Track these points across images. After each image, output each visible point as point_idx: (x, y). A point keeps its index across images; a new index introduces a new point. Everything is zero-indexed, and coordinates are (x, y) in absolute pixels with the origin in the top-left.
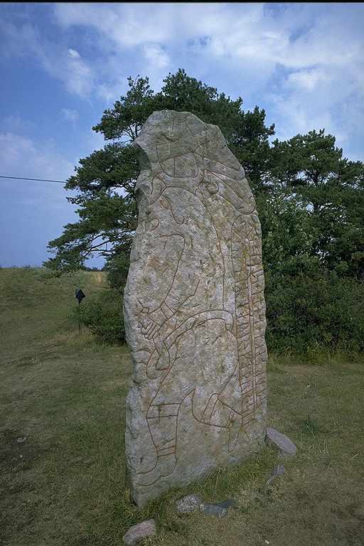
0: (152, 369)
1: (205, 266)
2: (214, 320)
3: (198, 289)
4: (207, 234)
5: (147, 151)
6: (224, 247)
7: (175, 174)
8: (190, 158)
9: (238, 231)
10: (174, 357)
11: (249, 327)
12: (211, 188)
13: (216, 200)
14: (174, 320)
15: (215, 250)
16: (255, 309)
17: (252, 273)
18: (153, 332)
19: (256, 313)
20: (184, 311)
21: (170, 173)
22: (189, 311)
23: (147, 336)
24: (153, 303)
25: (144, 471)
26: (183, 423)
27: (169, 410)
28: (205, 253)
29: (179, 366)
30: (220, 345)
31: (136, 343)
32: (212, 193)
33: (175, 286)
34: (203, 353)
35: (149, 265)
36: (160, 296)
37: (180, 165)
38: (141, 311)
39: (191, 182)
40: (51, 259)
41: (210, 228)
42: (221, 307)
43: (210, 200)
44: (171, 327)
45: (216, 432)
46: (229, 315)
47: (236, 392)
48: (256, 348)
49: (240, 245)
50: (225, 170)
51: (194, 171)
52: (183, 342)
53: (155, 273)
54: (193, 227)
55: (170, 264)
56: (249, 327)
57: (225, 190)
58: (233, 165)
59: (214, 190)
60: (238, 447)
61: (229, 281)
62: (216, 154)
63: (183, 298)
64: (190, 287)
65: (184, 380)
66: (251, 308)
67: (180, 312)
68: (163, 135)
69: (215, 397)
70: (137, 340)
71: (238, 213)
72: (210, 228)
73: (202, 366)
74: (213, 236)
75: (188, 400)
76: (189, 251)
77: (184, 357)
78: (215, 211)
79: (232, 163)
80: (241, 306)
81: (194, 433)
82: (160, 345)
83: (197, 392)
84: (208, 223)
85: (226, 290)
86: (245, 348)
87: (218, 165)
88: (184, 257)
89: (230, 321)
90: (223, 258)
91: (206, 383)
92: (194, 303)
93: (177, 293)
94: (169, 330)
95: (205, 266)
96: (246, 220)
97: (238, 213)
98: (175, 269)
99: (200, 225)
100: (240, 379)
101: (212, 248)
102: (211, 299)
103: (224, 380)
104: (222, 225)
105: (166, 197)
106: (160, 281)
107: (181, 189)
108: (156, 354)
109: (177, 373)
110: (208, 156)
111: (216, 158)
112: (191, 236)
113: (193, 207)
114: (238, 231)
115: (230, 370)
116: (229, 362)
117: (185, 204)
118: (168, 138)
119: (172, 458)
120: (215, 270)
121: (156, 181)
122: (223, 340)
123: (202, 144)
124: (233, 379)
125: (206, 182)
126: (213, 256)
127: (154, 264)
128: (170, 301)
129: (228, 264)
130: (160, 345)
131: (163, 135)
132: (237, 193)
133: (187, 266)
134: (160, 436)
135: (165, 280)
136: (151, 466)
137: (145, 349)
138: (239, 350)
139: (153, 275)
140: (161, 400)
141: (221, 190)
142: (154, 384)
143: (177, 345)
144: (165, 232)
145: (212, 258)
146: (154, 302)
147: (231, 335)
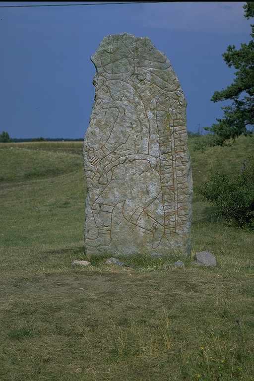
0: (95, 182)
1: (134, 126)
7: (113, 72)
8: (124, 61)
9: (162, 103)
11: (171, 168)
12: (141, 77)
13: (144, 84)
15: (142, 116)
16: (178, 156)
17: (175, 131)
19: (179, 160)
22: (121, 153)
24: (96, 146)
25: (90, 238)
26: (115, 218)
27: (106, 208)
29: (115, 185)
30: (146, 177)
32: (141, 81)
33: (111, 137)
34: (132, 179)
37: (117, 67)
40: (220, 121)
41: (139, 103)
43: (139, 85)
44: (109, 161)
45: (141, 232)
47: (159, 210)
48: (177, 184)
50: (152, 64)
51: (127, 69)
54: (126, 102)
56: (171, 168)
59: (142, 78)
60: (160, 247)
62: (144, 55)
65: (117, 193)
67: (115, 152)
68: (105, 51)
69: (141, 210)
70: (86, 165)
71: (163, 92)
72: (139, 103)
73: (131, 187)
74: (141, 107)
75: (120, 205)
78: (143, 91)
79: (158, 58)
80: (164, 153)
81: (124, 227)
82: (100, 170)
83: (127, 202)
84: (137, 99)
85: (151, 142)
87: (146, 62)
88: (118, 120)
89: (153, 161)
90: (149, 121)
91: (133, 198)
93: (112, 141)
95: (134, 126)
96: (170, 96)
97: (163, 92)
99: (131, 101)
100: (163, 203)
101: (140, 115)
103: (148, 200)
104: (149, 100)
105: (107, 86)
108: (98, 174)
109: (113, 188)
110: (138, 57)
112: (124, 109)
114: (162, 103)
115: (154, 194)
116: (153, 189)
119: (108, 237)
121: (100, 78)
122: (148, 174)
123: (133, 51)
124: (157, 201)
125: (136, 74)
127: (98, 125)
128: (108, 145)
129: (153, 125)
131: (105, 51)
132: (163, 79)
134: (100, 221)
136: (95, 237)
137: (91, 170)
139: (97, 130)
140: (101, 201)
141: (148, 78)
142: (97, 191)
143: (112, 171)
144: (105, 106)
146: (97, 145)
147: (155, 171)
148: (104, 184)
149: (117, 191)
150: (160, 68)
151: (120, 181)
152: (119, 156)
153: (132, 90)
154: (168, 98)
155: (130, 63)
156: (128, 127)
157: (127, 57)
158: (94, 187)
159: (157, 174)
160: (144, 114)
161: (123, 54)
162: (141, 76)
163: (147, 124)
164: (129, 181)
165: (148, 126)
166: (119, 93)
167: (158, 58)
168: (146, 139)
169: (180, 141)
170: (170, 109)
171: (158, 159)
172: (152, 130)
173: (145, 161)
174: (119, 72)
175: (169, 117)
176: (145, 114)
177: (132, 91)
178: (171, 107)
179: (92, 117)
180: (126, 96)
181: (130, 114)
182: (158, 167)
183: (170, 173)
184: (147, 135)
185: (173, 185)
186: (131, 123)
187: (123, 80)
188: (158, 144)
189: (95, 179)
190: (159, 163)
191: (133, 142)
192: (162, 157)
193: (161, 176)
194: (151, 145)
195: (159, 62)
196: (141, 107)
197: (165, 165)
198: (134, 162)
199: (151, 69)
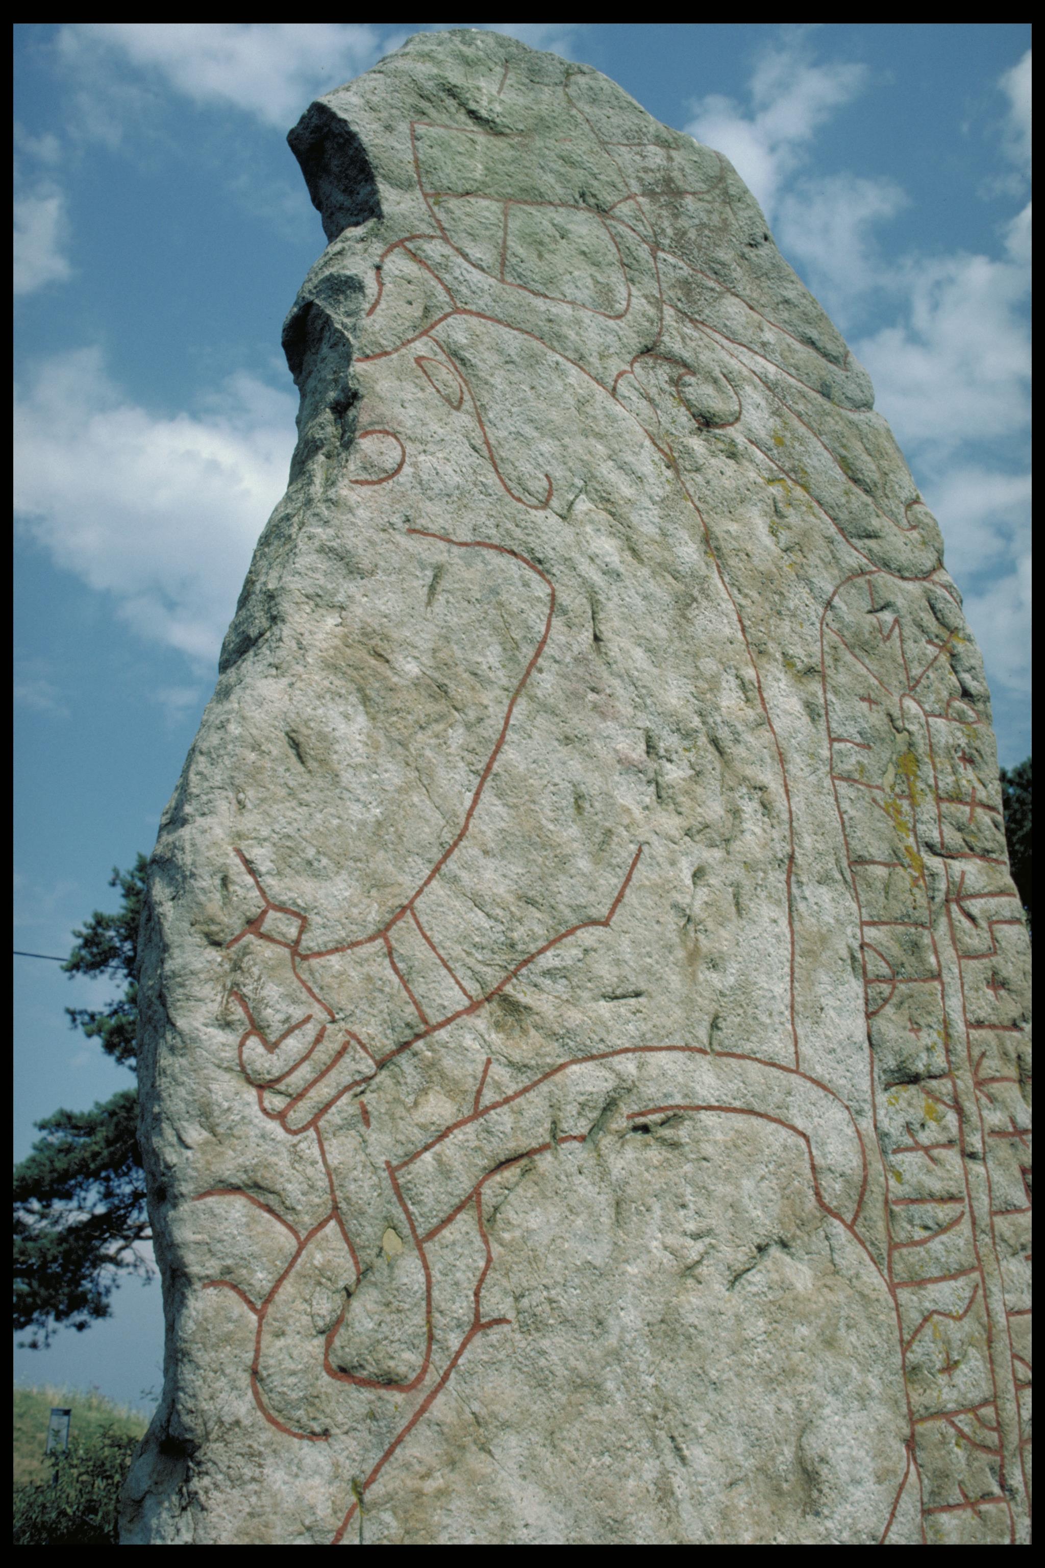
0: (294, 1354)
2: (740, 1122)
3: (631, 897)
4: (684, 604)
5: (367, 130)
6: (785, 698)
8: (584, 227)
10: (462, 1309)
13: (732, 455)
14: (473, 1042)
17: (958, 894)
18: (324, 1091)
20: (543, 1001)
21: (475, 252)
22: (574, 1017)
23: (277, 1102)
24: (335, 898)
28: (675, 695)
29: (503, 1390)
30: (783, 1308)
31: (195, 1134)
32: (706, 422)
34: (668, 1330)
35: (331, 666)
36: (382, 862)
37: (537, 244)
38: (253, 924)
39: (593, 332)
42: (778, 1045)
44: (453, 1089)
46: (838, 1115)
49: (876, 719)
52: (529, 1216)
53: (361, 720)
54: (608, 547)
55: (459, 692)
56: (965, 1227)
57: (773, 423)
58: (814, 334)
61: (827, 904)
63: (533, 926)
64: (583, 864)
66: (969, 1106)
67: (512, 1007)
70: (205, 1114)
71: (852, 558)
74: (717, 621)
76: (580, 660)
77: (533, 1324)
82: (365, 1189)
84: (689, 552)
85: (805, 950)
86: (950, 1367)
87: (732, 308)
88: (546, 682)
89: (839, 1151)
90: (782, 759)
92: (605, 971)
93: (496, 878)
94: (438, 1108)
95: (674, 774)
96: (900, 602)
97: (852, 558)
98: (490, 729)
99: (647, 550)
101: (714, 685)
102: (714, 977)
105: (455, 355)
106: (393, 774)
107: (536, 344)
108: (330, 1252)
109: (480, 1431)
111: (718, 271)
113: (600, 449)
114: (862, 646)
117: (555, 415)
118: (472, 114)
120: (735, 812)
122: (801, 1275)
123: (650, 193)
125: (671, 359)
126: (723, 733)
127: (365, 662)
128: (448, 914)
130: (365, 1189)
132: (845, 464)
133: (567, 740)
135: (424, 777)
137: (254, 1189)
138: (911, 1372)
141: (757, 417)
143: (488, 1223)
144: (435, 515)
145: (715, 742)
147: (852, 1255)
148: (390, 1382)
149: (529, 1469)
150: (825, 391)
151: (559, 1349)
152: (553, 1053)
153: (647, 460)
154: (887, 617)
155: (628, 265)
156: (628, 766)
157: (602, 211)
158: (278, 1416)
159: (873, 1280)
160: (743, 686)
161: (578, 176)
162: (709, 389)
163: (769, 777)
164: (643, 1354)
165: (780, 804)
166: (547, 446)
167: (807, 319)
168: (768, 915)
169: (997, 982)
170: (911, 705)
171: (866, 1124)
172: (808, 841)
173: (775, 1138)
174: (545, 288)
175: (908, 762)
176: (752, 692)
177: (647, 469)
178: (912, 687)
179: (294, 584)
180: (606, 500)
181: (639, 653)
182: (875, 1210)
183: (962, 1272)
184: (777, 877)
185: (992, 1400)
186: (651, 748)
187: (580, 360)
188: (855, 986)
189: (302, 1307)
190: (877, 1166)
191: (672, 921)
192: (896, 1110)
193: (904, 1295)
194: (812, 983)
195: (810, 342)
196: (717, 621)
197: (923, 1197)
198: (682, 1133)
199: (772, 369)
